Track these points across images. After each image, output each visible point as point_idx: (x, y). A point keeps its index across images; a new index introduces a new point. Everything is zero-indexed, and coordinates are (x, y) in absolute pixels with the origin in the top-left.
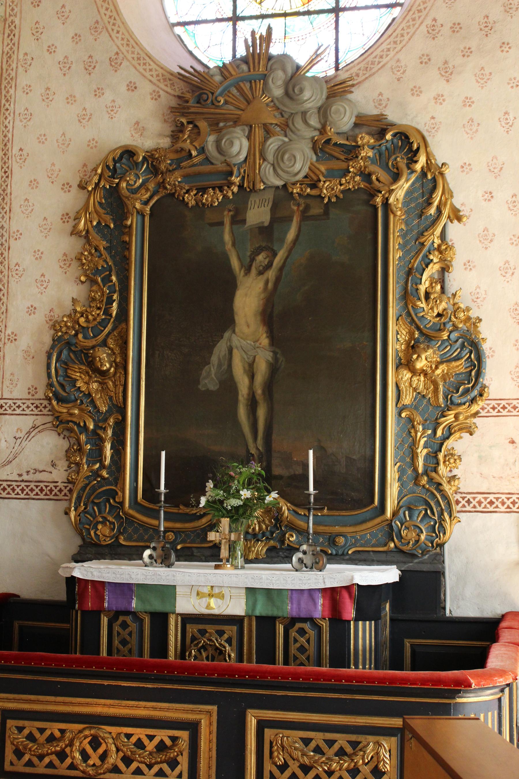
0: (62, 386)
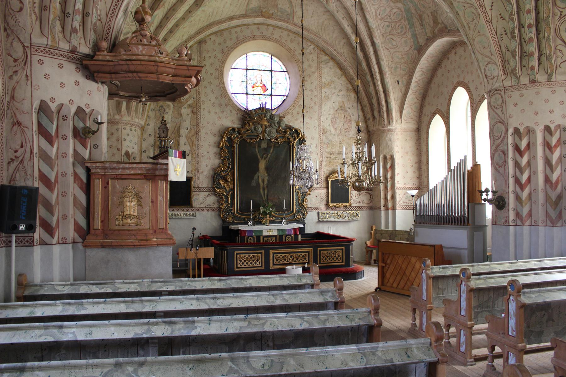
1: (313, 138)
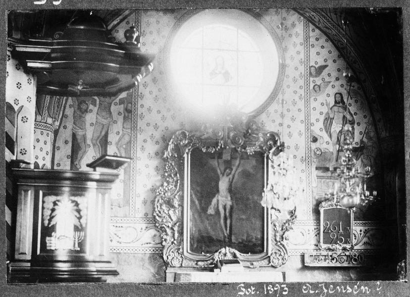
0: (160, 212)
1: (297, 148)
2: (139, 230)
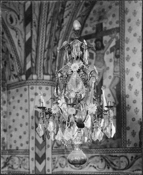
2: (130, 158)
